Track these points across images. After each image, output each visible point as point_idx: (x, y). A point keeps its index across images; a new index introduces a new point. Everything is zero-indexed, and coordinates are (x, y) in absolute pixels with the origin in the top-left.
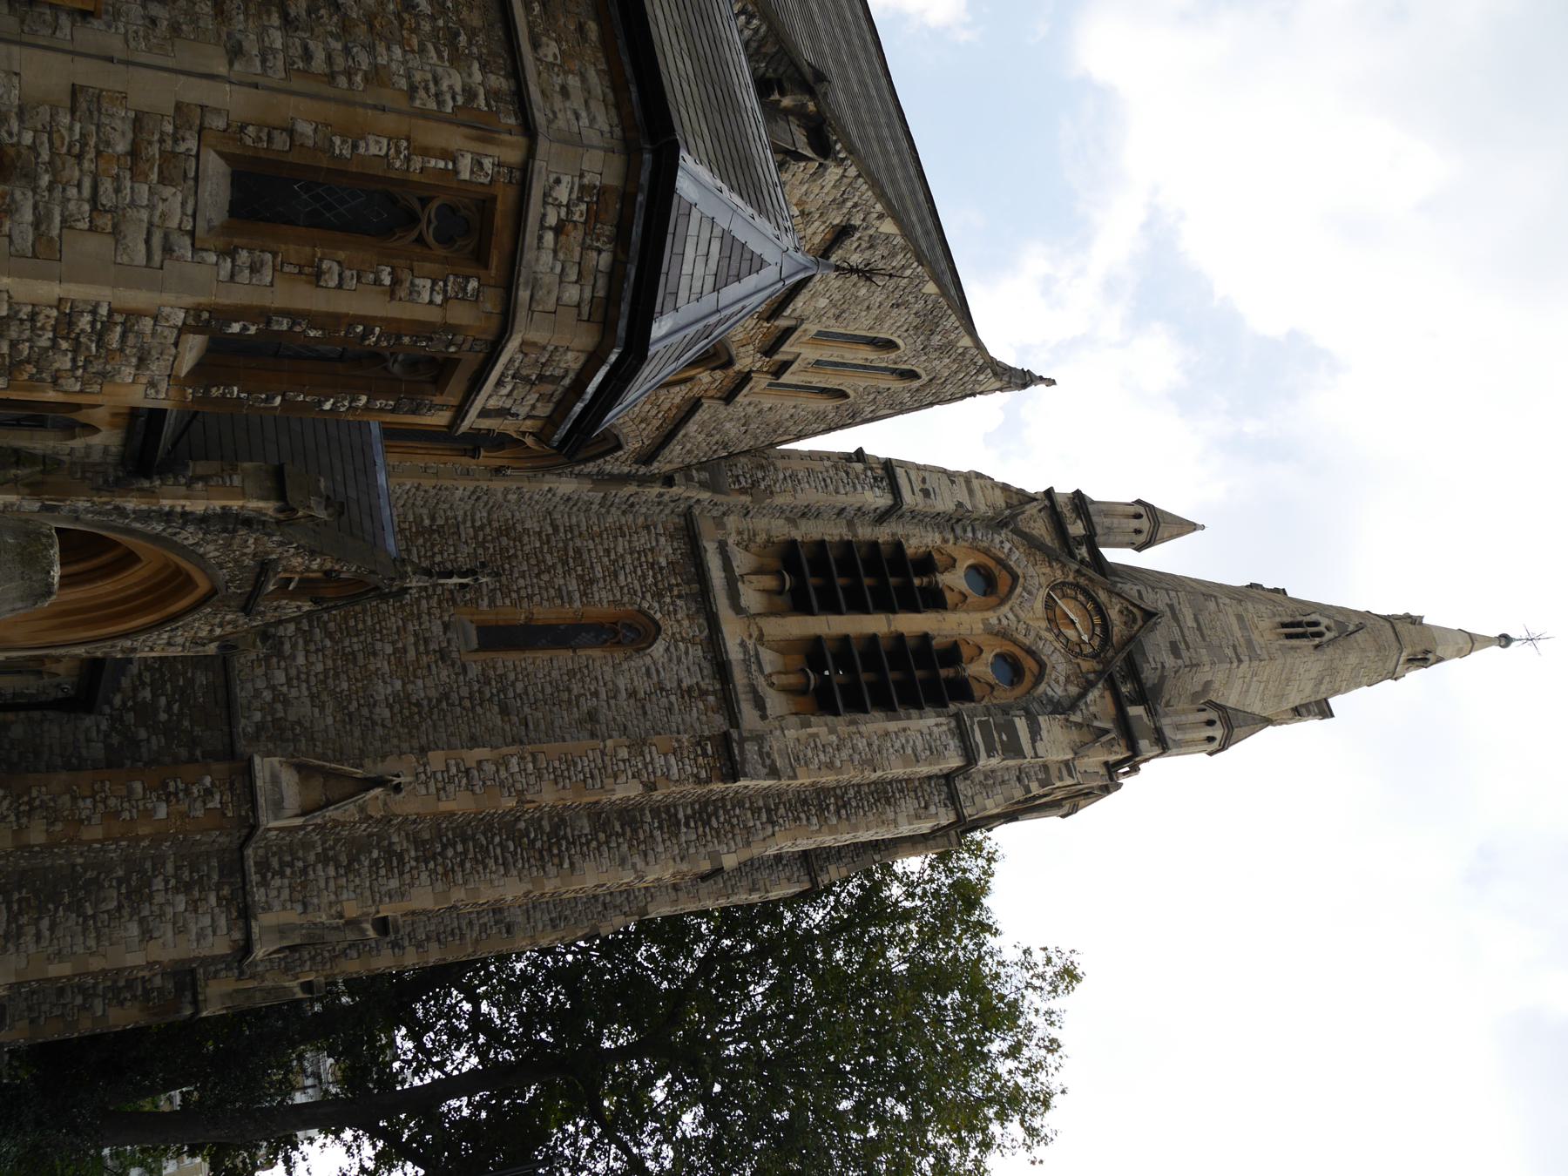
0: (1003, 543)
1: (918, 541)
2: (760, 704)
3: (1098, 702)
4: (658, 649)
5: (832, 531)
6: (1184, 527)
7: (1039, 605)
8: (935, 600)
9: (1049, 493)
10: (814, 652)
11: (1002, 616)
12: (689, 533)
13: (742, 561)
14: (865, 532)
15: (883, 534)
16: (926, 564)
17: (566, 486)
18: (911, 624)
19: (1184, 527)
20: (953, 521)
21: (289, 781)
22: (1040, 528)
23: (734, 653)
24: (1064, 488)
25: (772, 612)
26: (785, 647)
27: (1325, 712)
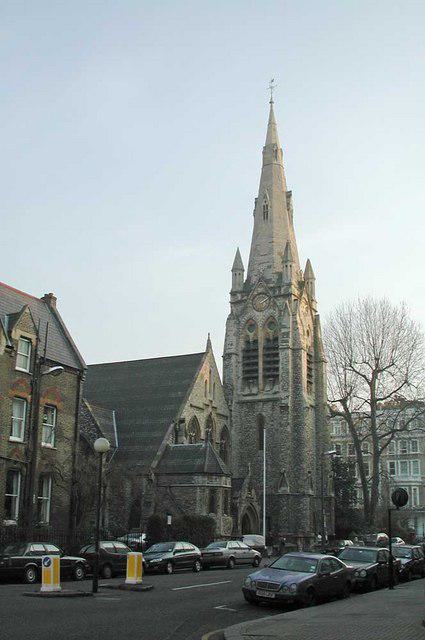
0: (243, 321)
1: (242, 345)
2: (275, 393)
3: (280, 302)
4: (264, 414)
5: (241, 368)
6: (238, 256)
7: (258, 313)
8: (256, 342)
9: (231, 303)
10: (265, 377)
11: (260, 324)
12: (242, 403)
13: (247, 392)
14: (240, 359)
15: (241, 354)
16: (248, 342)
17: (233, 432)
18: (261, 352)
19: (238, 256)
20: (237, 334)
21: (283, 489)
22: (240, 307)
23: (265, 397)
24: (228, 298)
25: (257, 385)
26: (265, 383)
27: (289, 195)
